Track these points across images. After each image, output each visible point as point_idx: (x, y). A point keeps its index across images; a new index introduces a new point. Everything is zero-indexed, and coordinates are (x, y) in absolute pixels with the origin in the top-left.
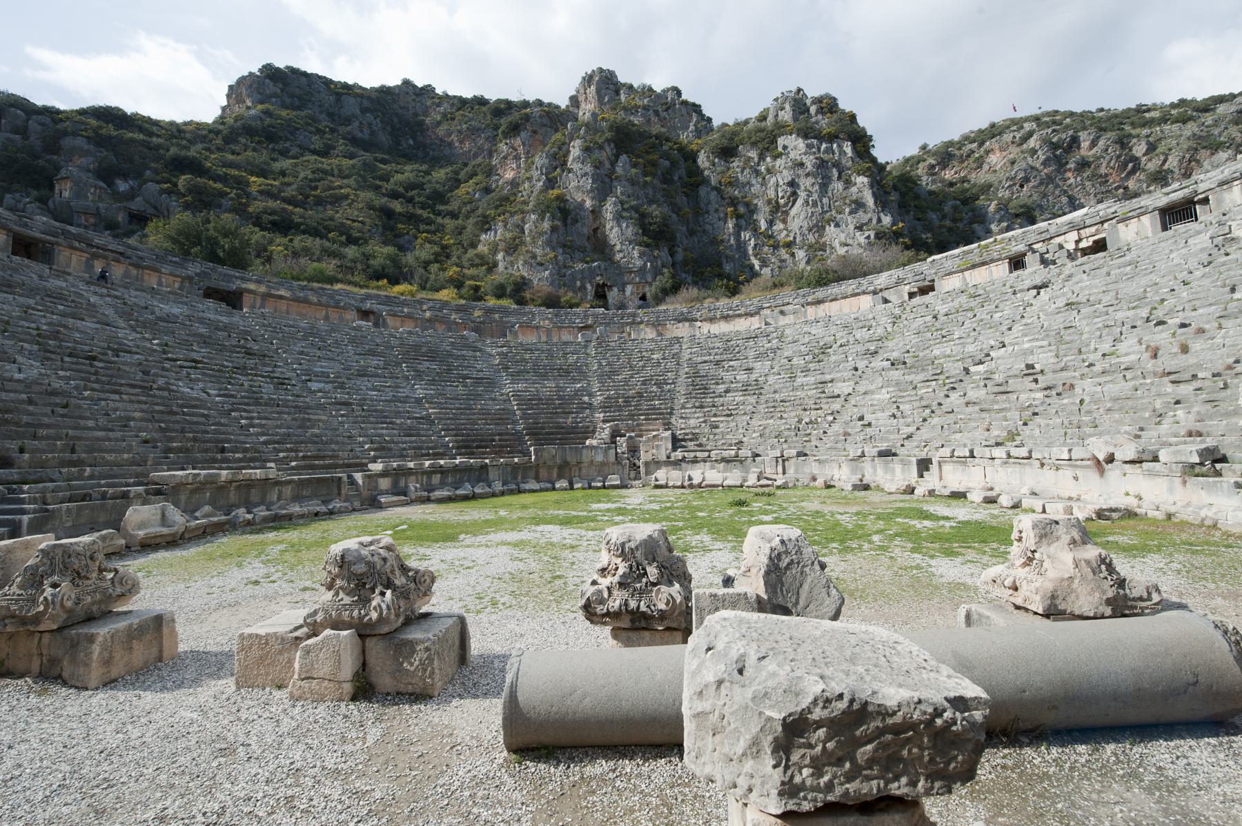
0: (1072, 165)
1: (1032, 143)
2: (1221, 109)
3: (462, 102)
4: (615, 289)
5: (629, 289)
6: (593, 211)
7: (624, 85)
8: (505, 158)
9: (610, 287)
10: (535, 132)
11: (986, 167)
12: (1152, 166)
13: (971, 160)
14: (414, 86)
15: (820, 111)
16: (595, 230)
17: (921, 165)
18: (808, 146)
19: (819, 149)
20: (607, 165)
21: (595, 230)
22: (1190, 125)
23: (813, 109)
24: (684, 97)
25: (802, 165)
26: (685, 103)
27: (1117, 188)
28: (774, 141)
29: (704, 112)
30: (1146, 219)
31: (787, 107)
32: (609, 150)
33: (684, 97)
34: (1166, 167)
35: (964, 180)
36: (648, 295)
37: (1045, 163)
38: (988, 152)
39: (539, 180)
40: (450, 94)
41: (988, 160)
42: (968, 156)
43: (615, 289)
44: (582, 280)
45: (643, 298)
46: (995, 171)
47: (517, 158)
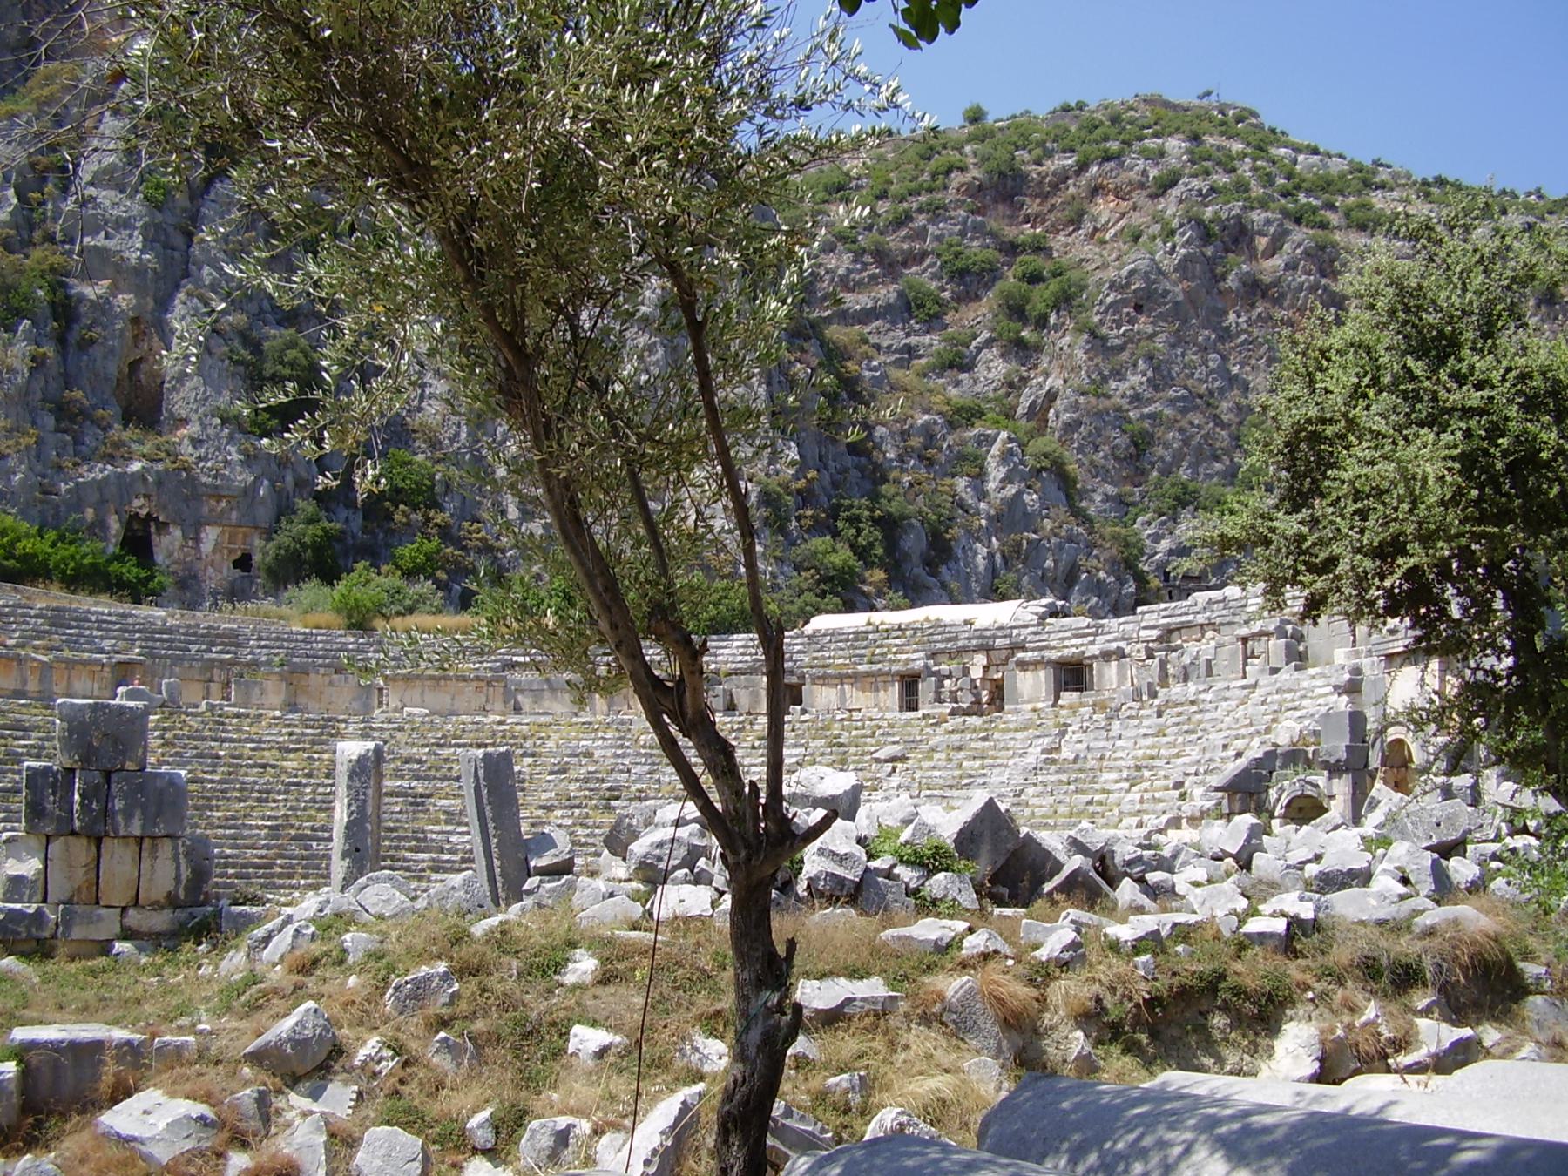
1: (1170, 205)
4: (177, 532)
5: (210, 535)
6: (135, 321)
9: (163, 527)
11: (1088, 226)
16: (134, 366)
17: (957, 179)
21: (134, 366)
30: (1042, 674)
35: (1040, 248)
36: (257, 558)
37: (1184, 266)
38: (1096, 190)
41: (1095, 210)
42: (1055, 187)
43: (177, 532)
44: (100, 505)
45: (244, 563)
46: (1103, 242)
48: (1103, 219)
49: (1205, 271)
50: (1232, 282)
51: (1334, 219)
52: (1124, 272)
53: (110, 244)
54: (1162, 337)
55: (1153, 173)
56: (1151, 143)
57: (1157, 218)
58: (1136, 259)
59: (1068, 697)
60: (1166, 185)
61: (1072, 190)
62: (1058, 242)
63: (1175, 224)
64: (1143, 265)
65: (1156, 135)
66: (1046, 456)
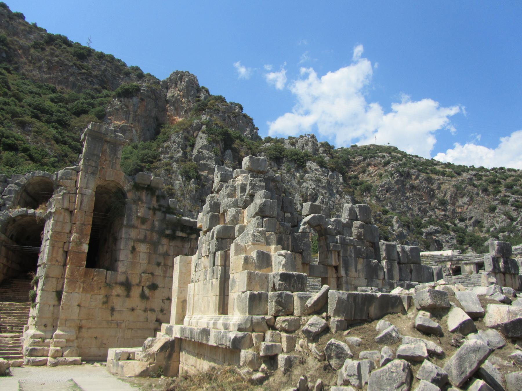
0: (408, 186)
1: (389, 168)
2: (464, 175)
3: (51, 39)
7: (203, 88)
8: (117, 110)
10: (142, 99)
11: (367, 173)
12: (440, 196)
13: (359, 166)
14: (9, 11)
15: (325, 152)
18: (323, 171)
19: (328, 174)
20: (220, 154)
22: (454, 179)
23: (321, 150)
24: (244, 112)
25: (319, 181)
26: (245, 116)
27: (426, 203)
28: (304, 162)
29: (254, 123)
30: (472, 266)
31: (310, 145)
32: (222, 145)
33: (244, 112)
34: (445, 198)
37: (397, 182)
38: (369, 165)
39: (178, 152)
40: (39, 25)
42: (358, 164)
46: (372, 177)
47: (127, 113)
48: (371, 171)
49: (402, 183)
50: (408, 186)
51: (428, 171)
52: (383, 183)
53: (208, 163)
54: (392, 198)
55: (383, 161)
56: (380, 154)
57: (386, 171)
58: (385, 181)
59: (480, 271)
60: (387, 163)
61: (362, 165)
62: (360, 176)
63: (393, 172)
64: (388, 181)
65: (380, 152)
66: (406, 221)
